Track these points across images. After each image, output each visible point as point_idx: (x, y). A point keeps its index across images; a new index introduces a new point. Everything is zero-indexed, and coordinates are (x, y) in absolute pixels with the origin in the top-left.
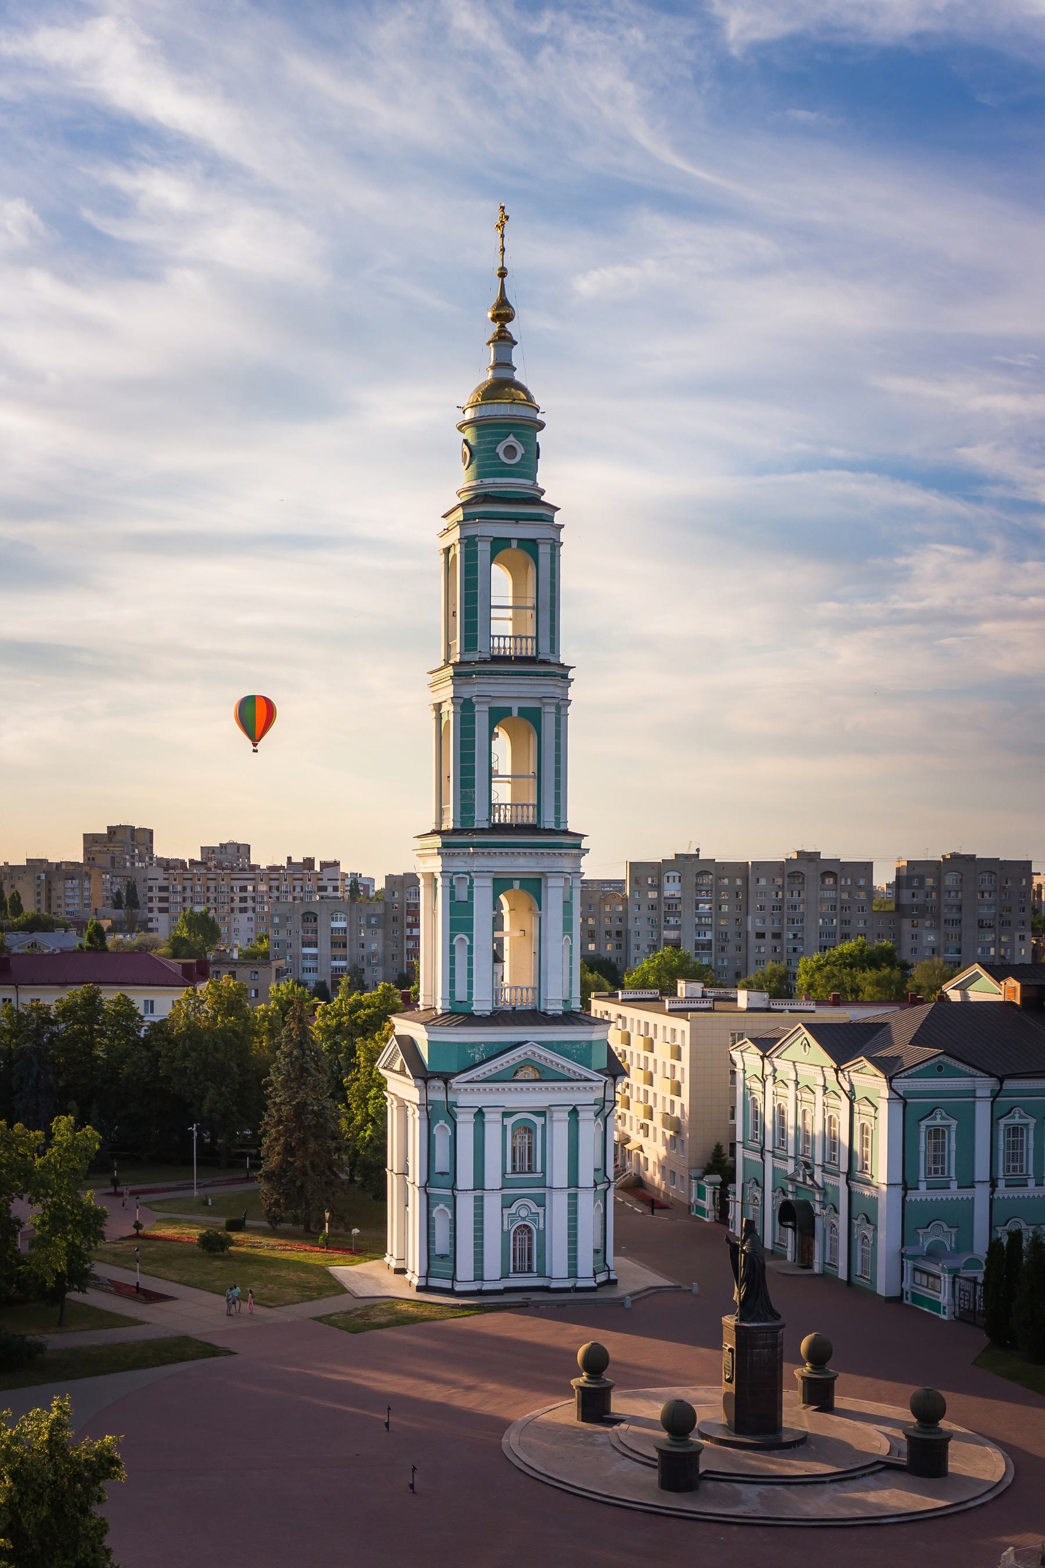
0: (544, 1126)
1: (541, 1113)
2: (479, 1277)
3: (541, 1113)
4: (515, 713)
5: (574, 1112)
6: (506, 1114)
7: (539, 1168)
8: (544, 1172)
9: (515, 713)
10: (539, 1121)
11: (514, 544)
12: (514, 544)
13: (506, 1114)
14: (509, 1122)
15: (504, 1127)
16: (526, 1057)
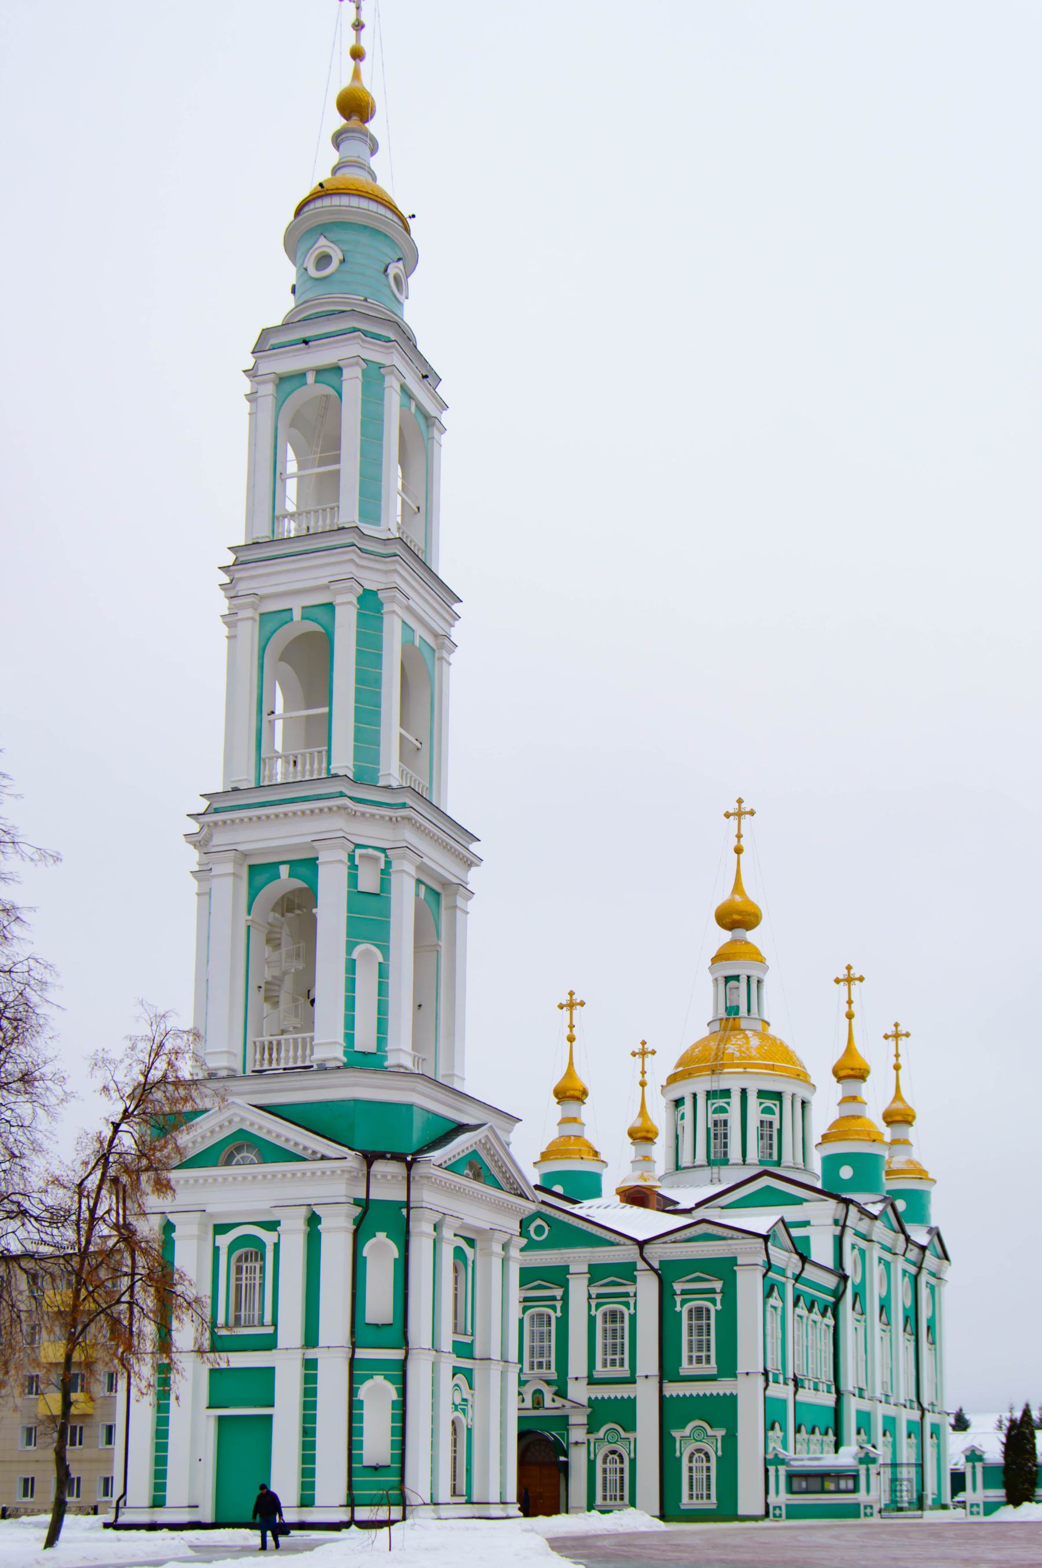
0: (277, 1246)
1: (272, 1226)
2: (158, 1502)
3: (272, 1226)
4: (297, 615)
5: (313, 1220)
6: (221, 1229)
7: (268, 1318)
8: (275, 1323)
9: (297, 615)
10: (268, 1238)
11: (311, 378)
12: (311, 378)
13: (221, 1229)
14: (224, 1241)
15: (216, 1250)
16: (234, 1129)
